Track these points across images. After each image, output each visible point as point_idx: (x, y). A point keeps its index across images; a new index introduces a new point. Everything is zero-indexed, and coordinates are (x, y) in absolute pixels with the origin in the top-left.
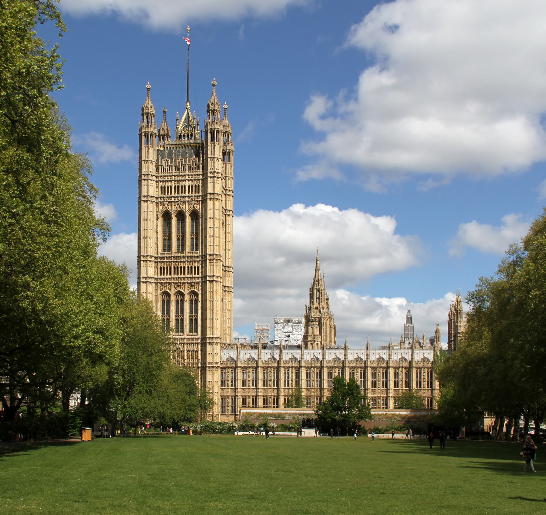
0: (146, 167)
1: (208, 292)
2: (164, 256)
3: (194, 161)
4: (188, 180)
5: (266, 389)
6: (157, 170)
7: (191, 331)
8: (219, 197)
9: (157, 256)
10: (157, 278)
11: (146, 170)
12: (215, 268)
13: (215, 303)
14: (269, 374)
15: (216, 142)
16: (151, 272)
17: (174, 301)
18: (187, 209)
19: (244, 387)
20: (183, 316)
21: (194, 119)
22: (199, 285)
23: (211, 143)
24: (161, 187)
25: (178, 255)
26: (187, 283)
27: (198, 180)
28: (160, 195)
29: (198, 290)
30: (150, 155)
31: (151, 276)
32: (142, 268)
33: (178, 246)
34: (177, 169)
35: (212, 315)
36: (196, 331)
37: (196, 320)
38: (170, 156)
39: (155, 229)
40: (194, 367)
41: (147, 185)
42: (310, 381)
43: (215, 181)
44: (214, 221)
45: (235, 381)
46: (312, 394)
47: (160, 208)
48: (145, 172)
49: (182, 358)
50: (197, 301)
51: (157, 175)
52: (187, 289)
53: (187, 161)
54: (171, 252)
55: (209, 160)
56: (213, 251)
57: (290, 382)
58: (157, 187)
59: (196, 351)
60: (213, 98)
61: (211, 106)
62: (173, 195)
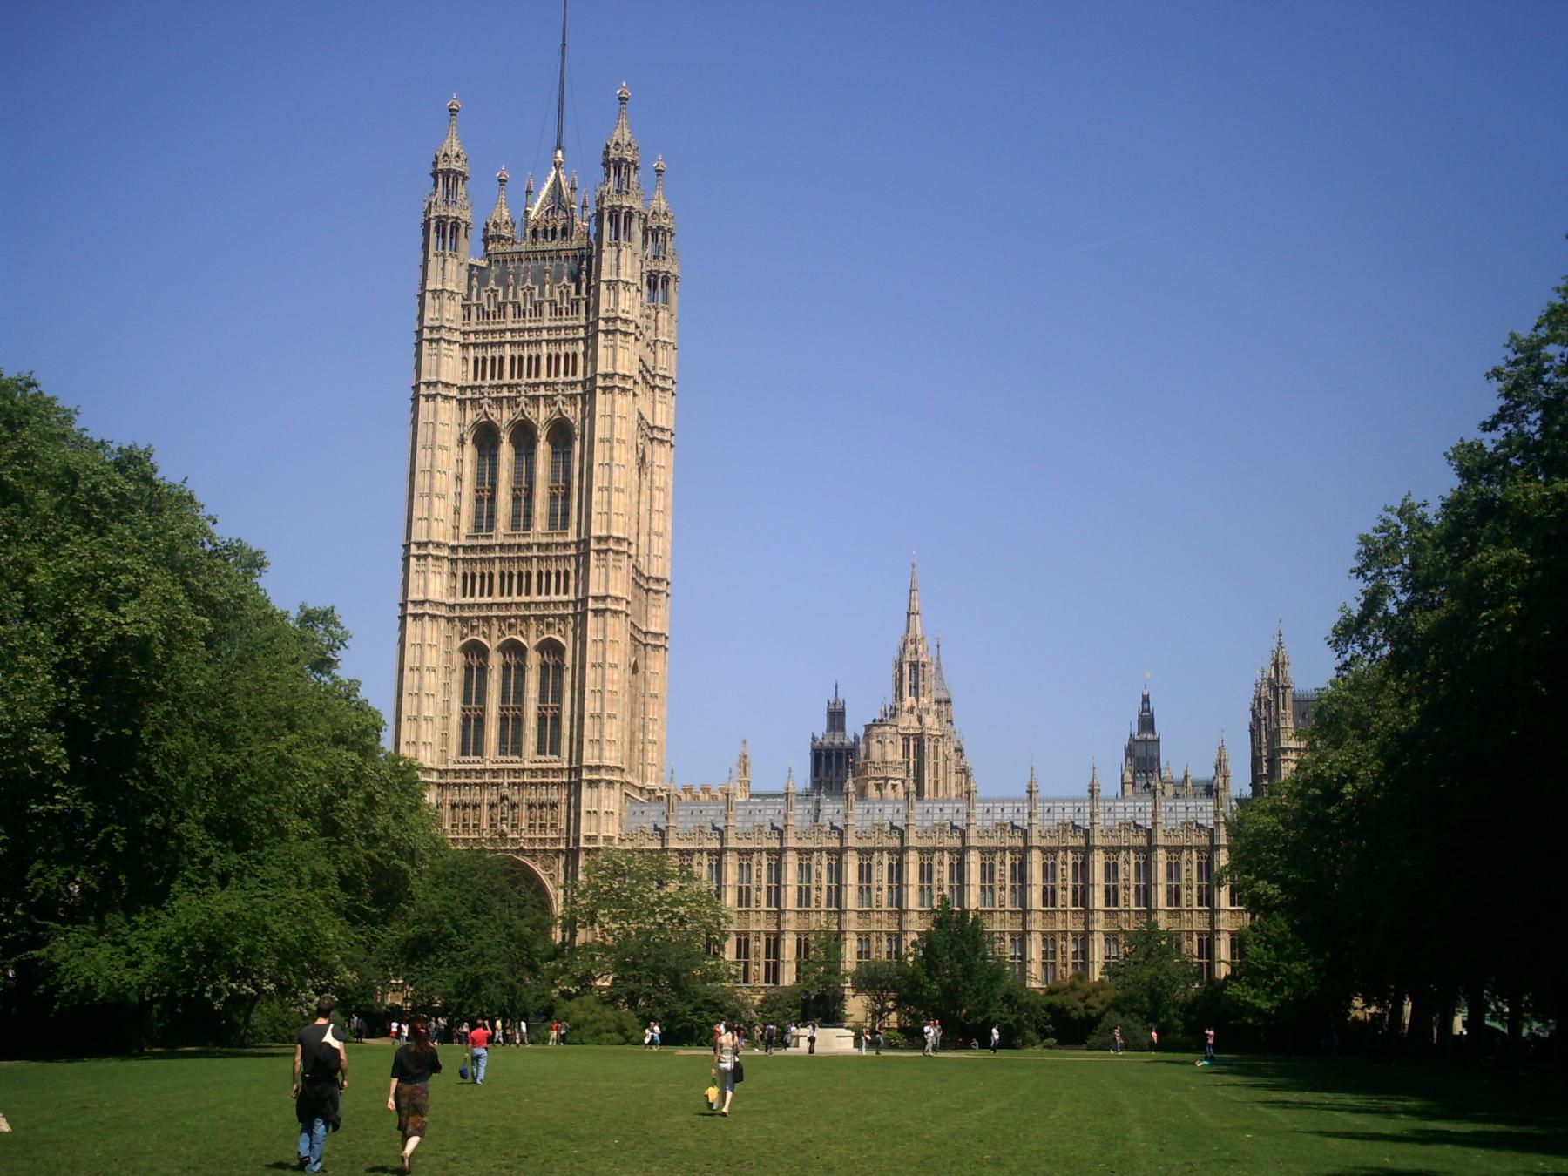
0: (437, 307)
2: (475, 542)
3: (565, 291)
4: (548, 342)
7: (541, 751)
8: (630, 385)
9: (455, 543)
10: (455, 605)
11: (437, 316)
12: (612, 574)
13: (608, 671)
14: (754, 869)
15: (622, 242)
16: (438, 588)
18: (542, 419)
21: (573, 189)
24: (476, 361)
25: (512, 541)
26: (535, 617)
27: (575, 341)
28: (471, 382)
29: (565, 636)
30: (448, 275)
34: (520, 312)
35: (598, 704)
36: (556, 750)
37: (557, 720)
38: (502, 281)
40: (546, 850)
42: (868, 888)
43: (619, 343)
44: (611, 448)
46: (875, 927)
48: (432, 319)
49: (513, 826)
50: (559, 668)
51: (467, 328)
53: (547, 292)
54: (493, 533)
55: (603, 286)
56: (608, 527)
57: (813, 896)
58: (465, 359)
59: (553, 806)
60: (618, 131)
61: (612, 151)
62: (507, 379)
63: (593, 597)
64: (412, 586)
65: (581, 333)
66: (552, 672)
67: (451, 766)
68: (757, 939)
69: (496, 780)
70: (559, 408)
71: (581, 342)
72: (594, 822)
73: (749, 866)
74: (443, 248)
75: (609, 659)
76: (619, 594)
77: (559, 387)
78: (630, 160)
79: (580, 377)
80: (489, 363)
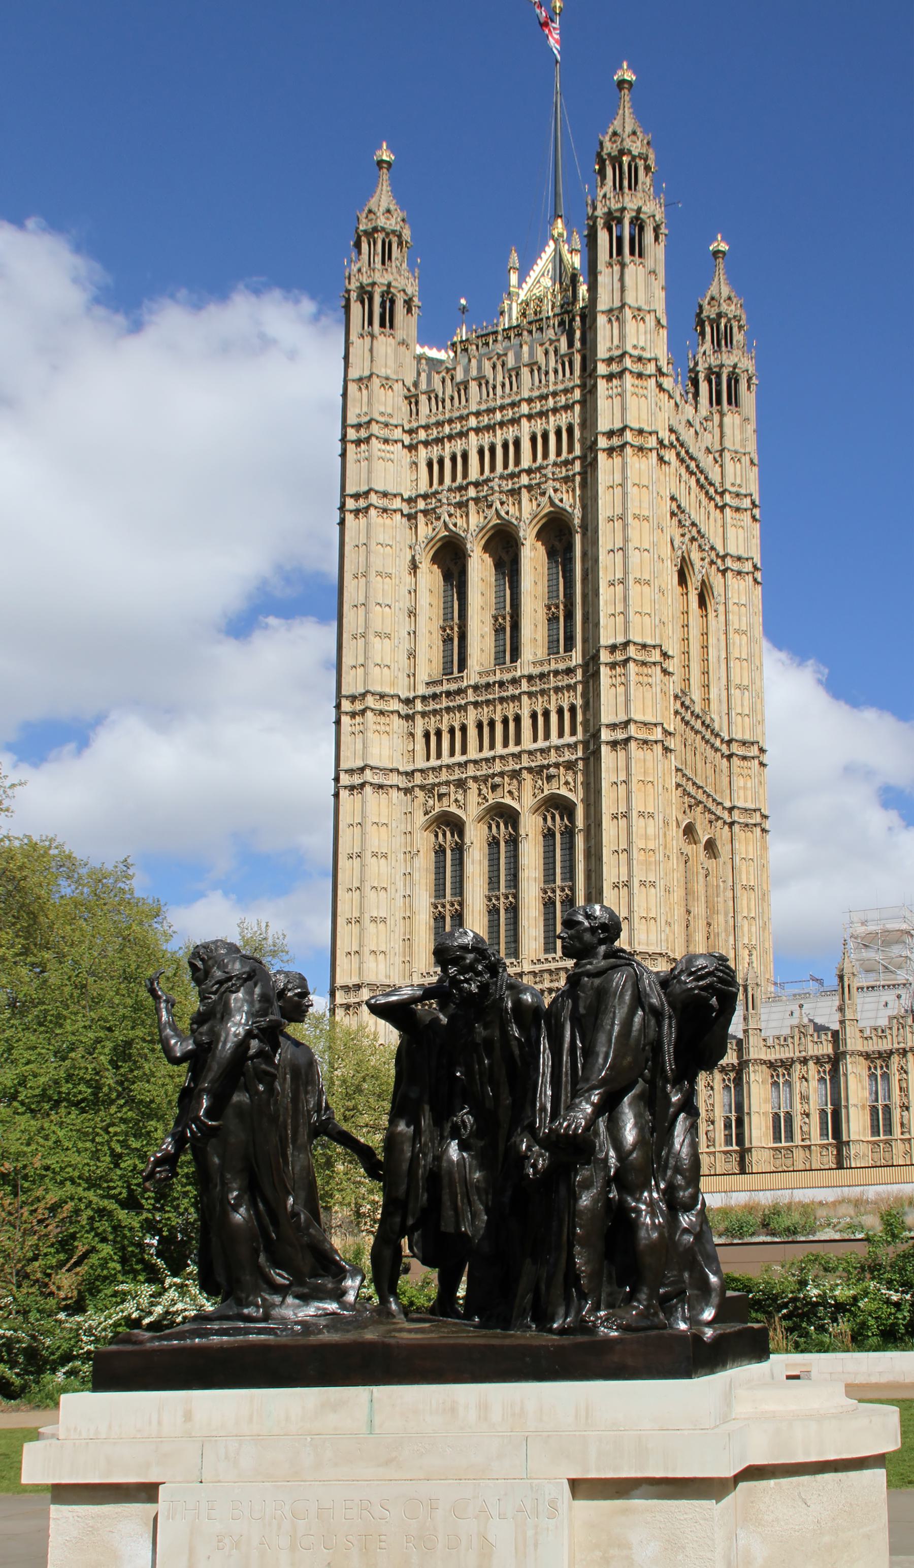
1: (605, 785)
5: (887, 1142)
10: (413, 772)
17: (477, 845)
19: (783, 1144)
20: (516, 896)
22: (575, 773)
23: (610, 265)
25: (491, 680)
26: (530, 770)
28: (423, 488)
29: (573, 790)
39: (405, 603)
44: (625, 527)
45: (740, 1122)
47: (424, 530)
50: (569, 834)
54: (464, 674)
63: (608, 726)
70: (550, 497)
73: (886, 1076)
75: (638, 805)
77: (549, 472)
78: (635, 153)
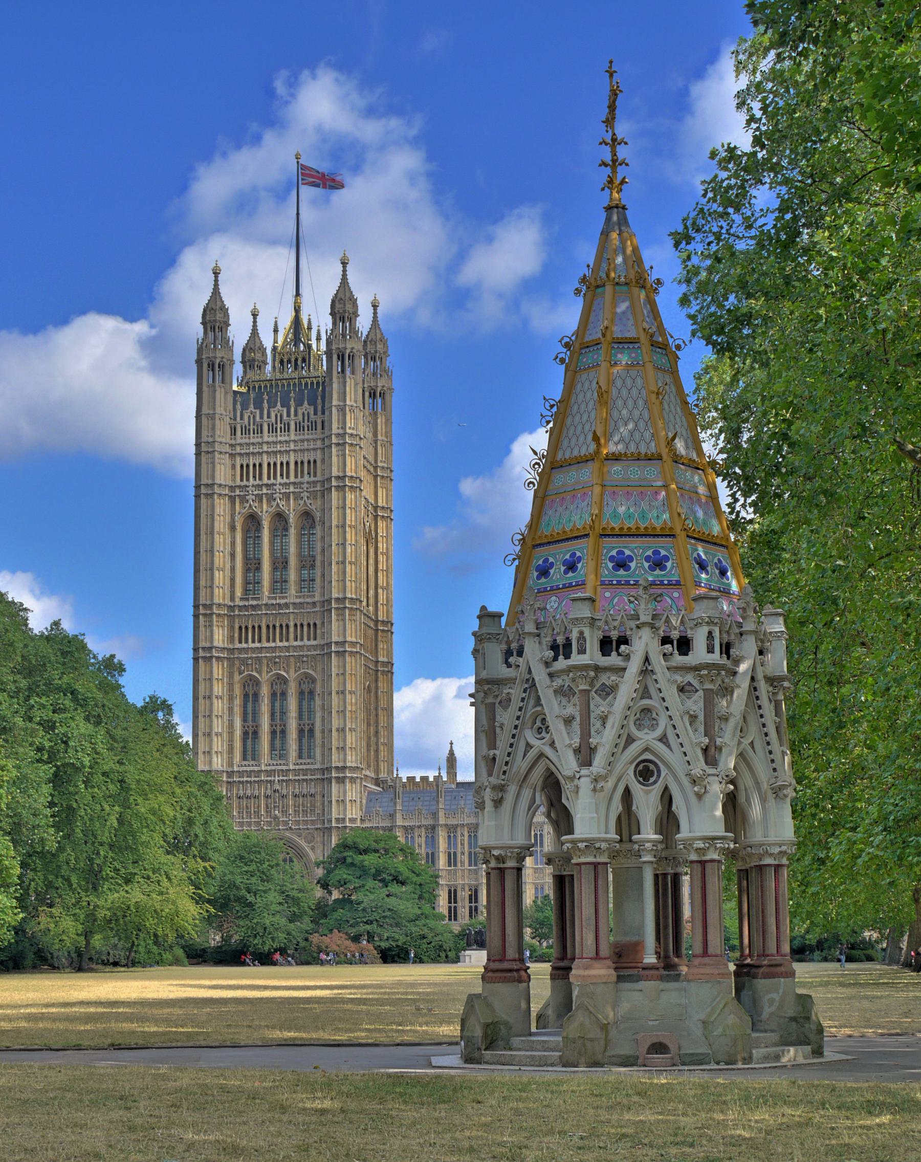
5: (455, 870)
6: (234, 431)
7: (300, 757)
13: (348, 697)
24: (242, 466)
27: (314, 449)
28: (238, 482)
31: (221, 645)
32: (202, 629)
33: (274, 582)
34: (272, 429)
35: (342, 721)
38: (258, 405)
41: (213, 463)
51: (233, 442)
52: (292, 671)
55: (334, 410)
58: (234, 467)
59: (311, 795)
62: (265, 480)
64: (202, 636)
65: (319, 444)
66: (306, 695)
67: (236, 769)
68: (463, 889)
69: (269, 779)
71: (319, 451)
72: (341, 808)
74: (214, 381)
76: (354, 640)
79: (319, 478)
80: (251, 467)
